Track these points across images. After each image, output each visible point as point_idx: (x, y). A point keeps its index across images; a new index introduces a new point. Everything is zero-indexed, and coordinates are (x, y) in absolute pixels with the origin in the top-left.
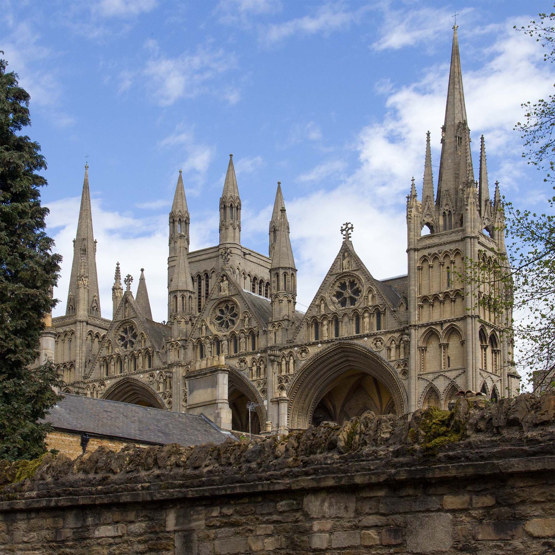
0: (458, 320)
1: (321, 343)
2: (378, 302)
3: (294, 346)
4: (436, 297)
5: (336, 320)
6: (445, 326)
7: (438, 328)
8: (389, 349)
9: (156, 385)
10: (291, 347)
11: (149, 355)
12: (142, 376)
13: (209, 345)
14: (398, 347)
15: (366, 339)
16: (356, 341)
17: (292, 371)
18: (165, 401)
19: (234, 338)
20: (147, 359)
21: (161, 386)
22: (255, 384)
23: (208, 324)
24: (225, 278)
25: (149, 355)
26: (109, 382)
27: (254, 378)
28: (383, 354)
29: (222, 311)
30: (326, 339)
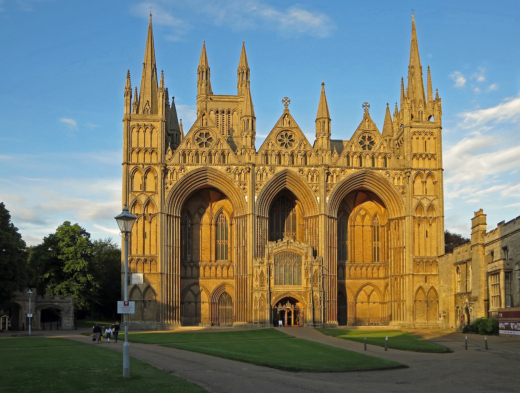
0: (434, 170)
1: (355, 168)
2: (386, 151)
3: (338, 167)
4: (421, 155)
6: (427, 172)
7: (423, 172)
9: (233, 175)
12: (220, 168)
14: (399, 179)
15: (381, 171)
16: (375, 171)
17: (334, 182)
18: (242, 187)
19: (292, 155)
21: (237, 176)
22: (310, 185)
23: (274, 142)
26: (189, 168)
27: (310, 182)
28: (391, 180)
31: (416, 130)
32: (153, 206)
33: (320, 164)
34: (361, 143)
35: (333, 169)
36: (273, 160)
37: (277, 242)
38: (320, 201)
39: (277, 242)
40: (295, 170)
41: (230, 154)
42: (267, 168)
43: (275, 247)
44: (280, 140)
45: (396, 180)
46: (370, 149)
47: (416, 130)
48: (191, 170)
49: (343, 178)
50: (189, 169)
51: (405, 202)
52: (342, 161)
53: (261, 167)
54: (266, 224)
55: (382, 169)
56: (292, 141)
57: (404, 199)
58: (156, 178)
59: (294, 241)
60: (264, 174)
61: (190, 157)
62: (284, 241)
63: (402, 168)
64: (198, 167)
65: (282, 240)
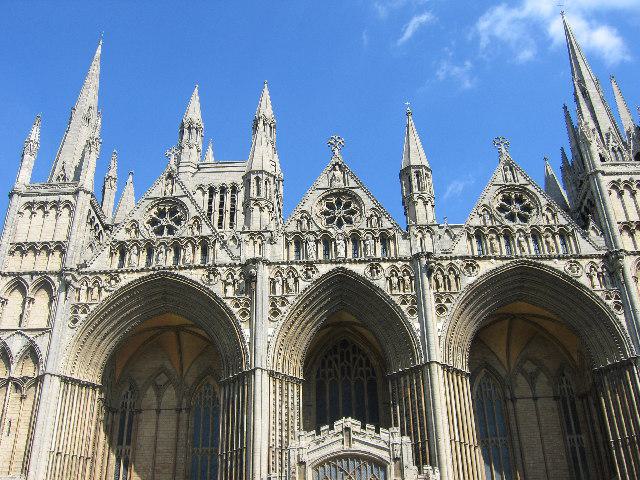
1: (495, 258)
2: (563, 221)
3: (456, 258)
5: (508, 236)
8: (591, 278)
10: (451, 258)
11: (205, 245)
13: (313, 243)
16: (545, 262)
17: (454, 289)
19: (355, 238)
20: (199, 251)
22: (397, 300)
24: (337, 167)
25: (205, 245)
28: (584, 280)
29: (330, 206)
30: (498, 254)
31: (615, 178)
32: (36, 360)
33: (414, 252)
34: (502, 209)
35: (449, 262)
36: (316, 252)
37: (318, 433)
38: (423, 332)
39: (318, 433)
40: (360, 269)
41: (218, 245)
42: (298, 268)
43: (314, 446)
44: (325, 213)
45: (595, 279)
46: (524, 219)
47: (615, 178)
48: (130, 280)
49: (471, 280)
50: (126, 279)
51: (624, 324)
52: (464, 247)
53: (285, 266)
54: (295, 395)
55: (559, 258)
56: (353, 212)
57: (622, 318)
58: (52, 299)
59: (363, 427)
60: (291, 281)
61: (134, 257)
62: (338, 428)
63: (603, 252)
64: (145, 274)
65: (332, 428)
